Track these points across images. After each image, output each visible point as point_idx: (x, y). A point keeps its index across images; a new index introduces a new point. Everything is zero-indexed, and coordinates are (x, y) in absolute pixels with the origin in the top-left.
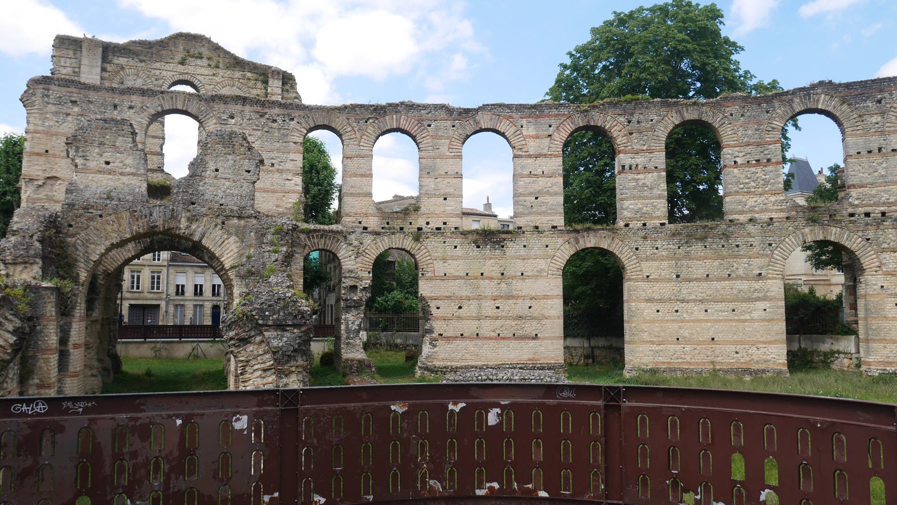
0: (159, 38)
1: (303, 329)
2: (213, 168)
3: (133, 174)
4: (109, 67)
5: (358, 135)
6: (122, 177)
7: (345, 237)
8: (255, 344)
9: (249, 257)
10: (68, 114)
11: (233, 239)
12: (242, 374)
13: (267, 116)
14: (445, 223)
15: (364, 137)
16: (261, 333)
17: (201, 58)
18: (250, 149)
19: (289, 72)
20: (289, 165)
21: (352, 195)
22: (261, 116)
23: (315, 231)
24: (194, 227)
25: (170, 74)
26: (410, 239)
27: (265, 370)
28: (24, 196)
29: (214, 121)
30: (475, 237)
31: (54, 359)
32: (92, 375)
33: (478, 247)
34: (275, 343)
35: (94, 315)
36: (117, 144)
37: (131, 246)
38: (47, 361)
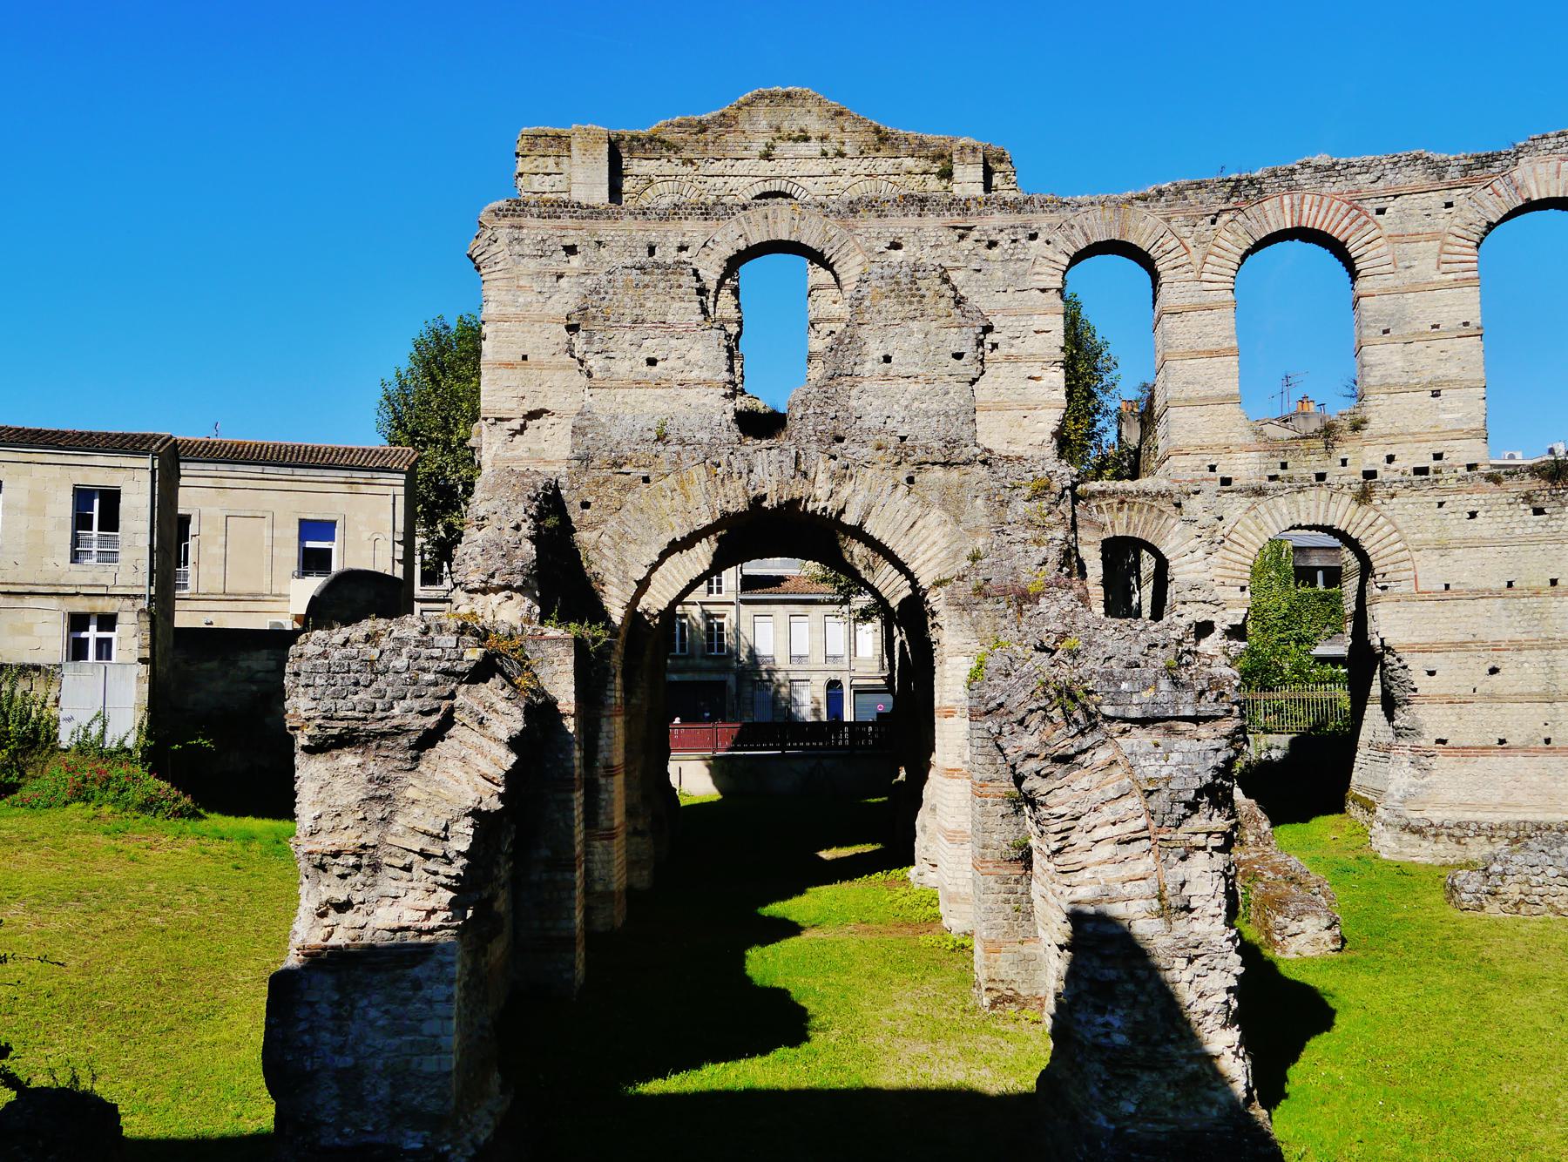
1: (1227, 726)
2: (880, 354)
5: (1196, 255)
6: (683, 391)
7: (1178, 505)
8: (1095, 770)
9: (975, 558)
10: (560, 277)
11: (936, 514)
13: (974, 234)
14: (1438, 457)
15: (1211, 258)
17: (807, 139)
18: (959, 302)
20: (1035, 344)
22: (962, 237)
23: (1103, 493)
24: (846, 490)
26: (1347, 499)
28: (485, 458)
29: (859, 258)
30: (1530, 484)
33: (1538, 511)
34: (1151, 768)
36: (670, 318)
38: (567, 806)
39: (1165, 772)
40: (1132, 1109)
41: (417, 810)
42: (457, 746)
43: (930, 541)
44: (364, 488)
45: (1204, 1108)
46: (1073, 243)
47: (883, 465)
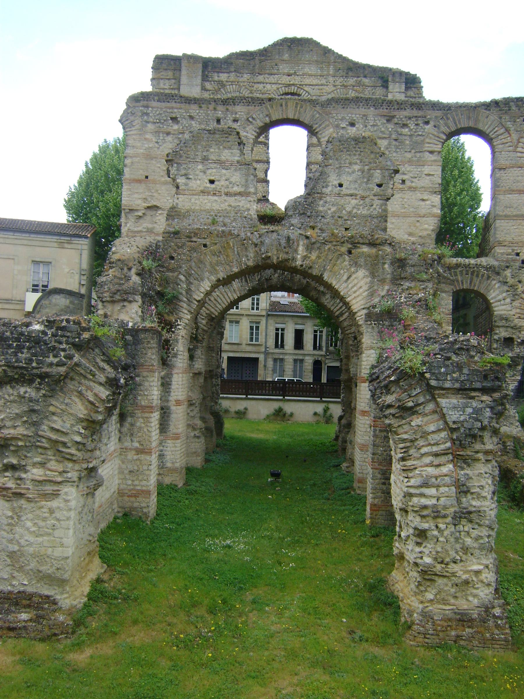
0: (261, 47)
2: (336, 183)
3: (240, 194)
4: (208, 85)
10: (168, 134)
11: (361, 273)
12: (403, 459)
13: (396, 120)
16: (434, 398)
19: (412, 72)
20: (426, 182)
21: (507, 217)
22: (388, 121)
23: (458, 265)
25: (275, 87)
27: (436, 455)
31: (156, 416)
32: (195, 436)
34: (453, 416)
35: (196, 366)
36: (223, 158)
37: (236, 284)
38: (147, 420)
39: (462, 418)
40: (431, 597)
41: (55, 418)
42: (77, 385)
43: (359, 285)
44: (66, 245)
45: (470, 598)
46: (448, 127)
47: (334, 243)
